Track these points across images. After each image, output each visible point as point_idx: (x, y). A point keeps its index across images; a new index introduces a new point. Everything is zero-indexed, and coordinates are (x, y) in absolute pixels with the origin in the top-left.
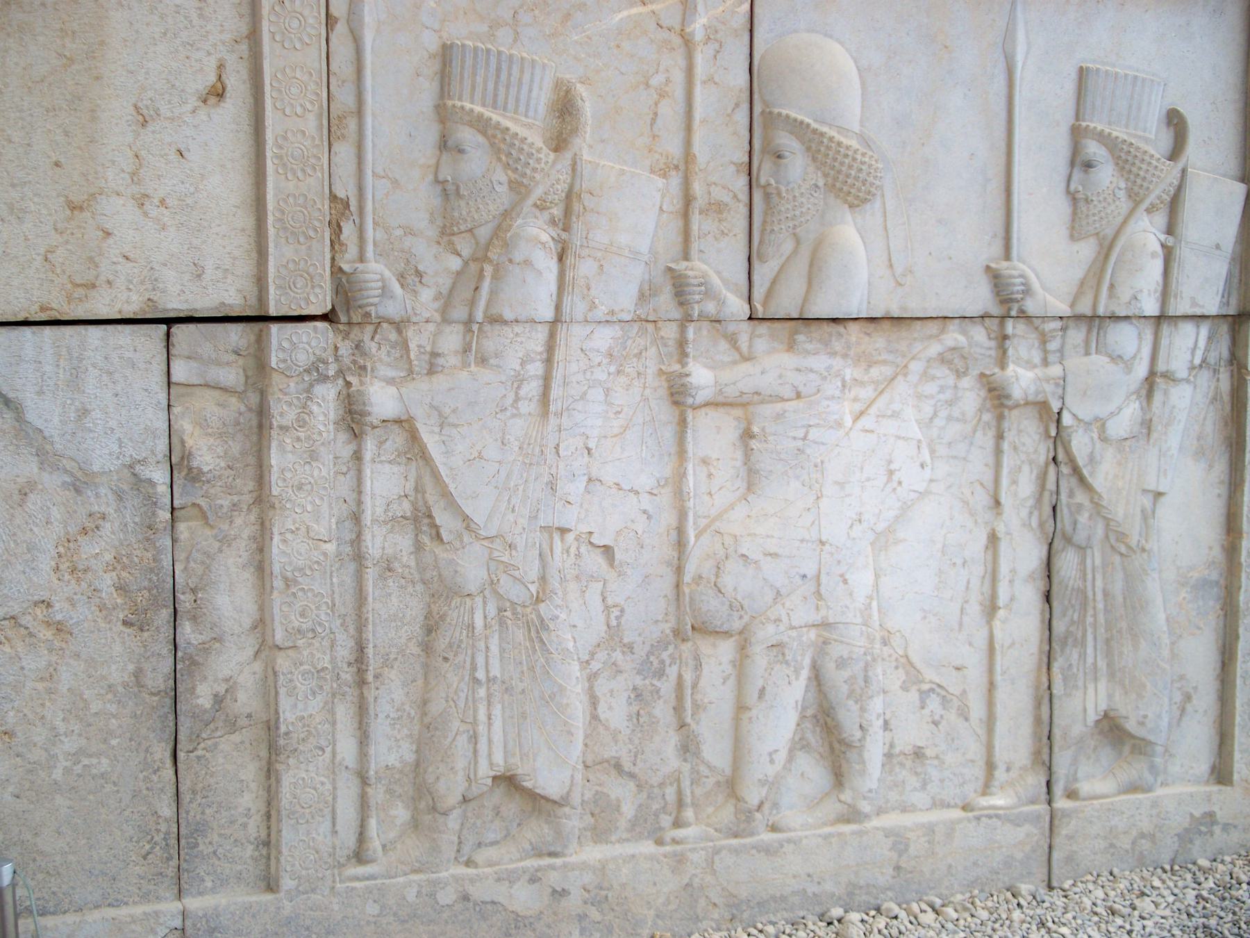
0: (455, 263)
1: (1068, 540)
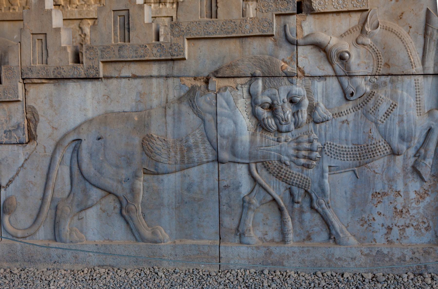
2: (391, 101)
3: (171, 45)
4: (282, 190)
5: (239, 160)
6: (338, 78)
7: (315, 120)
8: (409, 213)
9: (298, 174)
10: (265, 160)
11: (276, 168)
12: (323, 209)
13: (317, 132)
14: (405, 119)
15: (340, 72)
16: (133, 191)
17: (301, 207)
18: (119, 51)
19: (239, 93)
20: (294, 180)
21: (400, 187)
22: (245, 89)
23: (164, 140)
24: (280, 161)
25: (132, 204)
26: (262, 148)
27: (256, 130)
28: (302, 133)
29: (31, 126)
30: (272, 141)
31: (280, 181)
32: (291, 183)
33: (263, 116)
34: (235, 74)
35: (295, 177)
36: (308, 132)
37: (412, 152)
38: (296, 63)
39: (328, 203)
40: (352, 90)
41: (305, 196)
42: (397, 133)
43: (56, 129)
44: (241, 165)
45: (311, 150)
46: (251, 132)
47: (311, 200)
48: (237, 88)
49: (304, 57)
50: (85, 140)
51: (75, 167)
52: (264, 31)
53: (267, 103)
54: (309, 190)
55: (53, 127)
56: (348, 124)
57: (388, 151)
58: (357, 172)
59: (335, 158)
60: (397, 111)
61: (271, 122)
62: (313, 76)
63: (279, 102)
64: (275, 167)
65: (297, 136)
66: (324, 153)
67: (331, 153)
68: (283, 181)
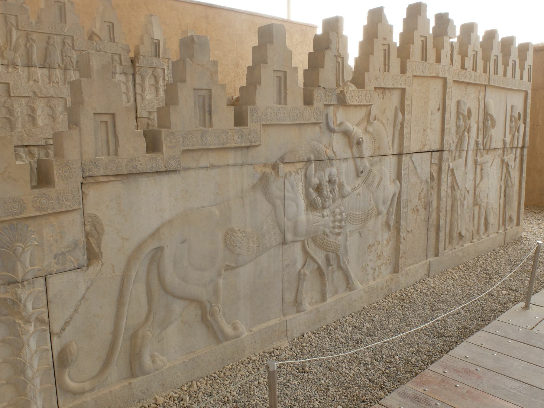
0: (457, 140)
1: (508, 186)
3: (250, 131)
6: (354, 160)
12: (346, 266)
16: (216, 292)
18: (201, 137)
21: (380, 239)
22: (303, 173)
23: (244, 231)
25: (216, 306)
29: (91, 241)
34: (297, 159)
37: (385, 211)
42: (382, 198)
43: (127, 239)
50: (167, 246)
51: (155, 282)
54: (339, 254)
55: (123, 238)
68: (324, 250)
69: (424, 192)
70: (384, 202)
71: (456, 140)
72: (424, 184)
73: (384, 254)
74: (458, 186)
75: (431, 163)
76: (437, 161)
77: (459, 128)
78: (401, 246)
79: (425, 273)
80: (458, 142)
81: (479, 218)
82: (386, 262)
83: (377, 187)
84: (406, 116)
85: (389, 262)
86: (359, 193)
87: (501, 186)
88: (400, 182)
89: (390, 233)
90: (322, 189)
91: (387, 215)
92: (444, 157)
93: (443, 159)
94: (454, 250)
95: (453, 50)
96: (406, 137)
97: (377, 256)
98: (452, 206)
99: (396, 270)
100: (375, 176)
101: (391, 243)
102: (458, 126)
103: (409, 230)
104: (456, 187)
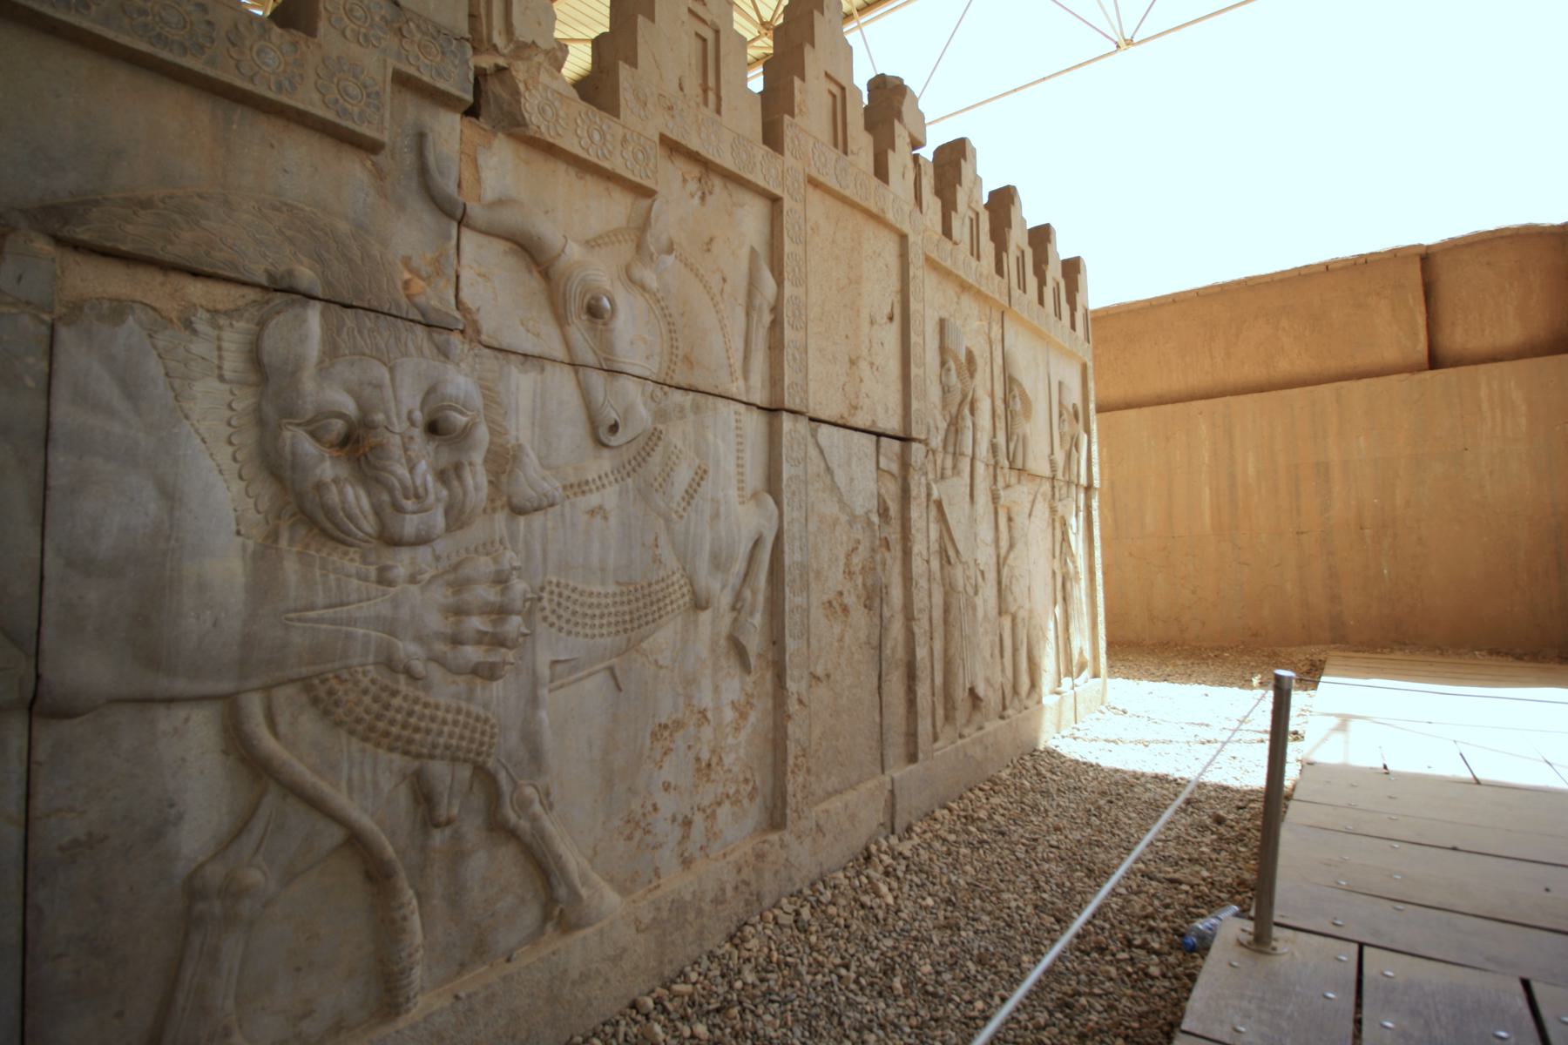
2: (697, 461)
4: (387, 783)
5: (182, 686)
6: (577, 373)
7: (515, 501)
8: (723, 766)
9: (454, 705)
10: (316, 669)
11: (367, 700)
12: (534, 819)
13: (521, 545)
14: (722, 509)
15: (587, 355)
17: (457, 837)
19: (199, 347)
20: (440, 734)
21: (706, 699)
22: (234, 338)
24: (390, 664)
26: (312, 614)
27: (274, 536)
28: (472, 548)
30: (355, 582)
31: (381, 751)
32: (425, 751)
33: (318, 471)
35: (444, 722)
36: (492, 543)
37: (725, 600)
38: (454, 285)
39: (548, 794)
40: (614, 416)
41: (471, 788)
42: (707, 547)
44: (181, 712)
45: (501, 612)
46: (251, 544)
47: (494, 797)
48: (188, 325)
49: (479, 275)
52: (345, 113)
53: (341, 416)
56: (606, 518)
57: (687, 598)
58: (618, 673)
59: (569, 633)
60: (707, 488)
61: (357, 498)
62: (505, 346)
63: (395, 420)
64: (365, 692)
65: (455, 559)
66: (538, 616)
67: (559, 617)
69: (863, 551)
70: (718, 563)
71: (943, 425)
72: (859, 526)
73: (729, 759)
74: (957, 552)
75: (878, 468)
76: (895, 467)
77: (949, 391)
78: (791, 728)
79: (882, 821)
80: (947, 431)
81: (1015, 650)
82: (738, 791)
83: (683, 499)
84: (788, 289)
85: (749, 788)
86: (601, 507)
87: (1054, 573)
88: (778, 503)
89: (749, 679)
90: (379, 448)
91: (734, 614)
92: (913, 459)
93: (913, 463)
94: (960, 742)
95: (920, 174)
96: (790, 357)
97: (698, 770)
98: (947, 610)
99: (776, 818)
100: (674, 457)
101: (753, 717)
102: (946, 388)
103: (820, 671)
104: (951, 553)
